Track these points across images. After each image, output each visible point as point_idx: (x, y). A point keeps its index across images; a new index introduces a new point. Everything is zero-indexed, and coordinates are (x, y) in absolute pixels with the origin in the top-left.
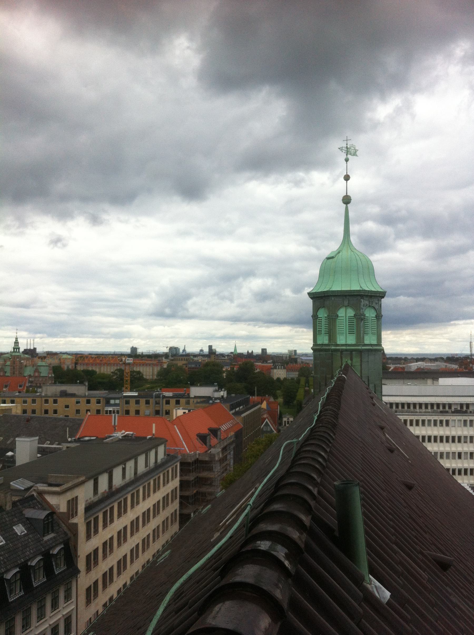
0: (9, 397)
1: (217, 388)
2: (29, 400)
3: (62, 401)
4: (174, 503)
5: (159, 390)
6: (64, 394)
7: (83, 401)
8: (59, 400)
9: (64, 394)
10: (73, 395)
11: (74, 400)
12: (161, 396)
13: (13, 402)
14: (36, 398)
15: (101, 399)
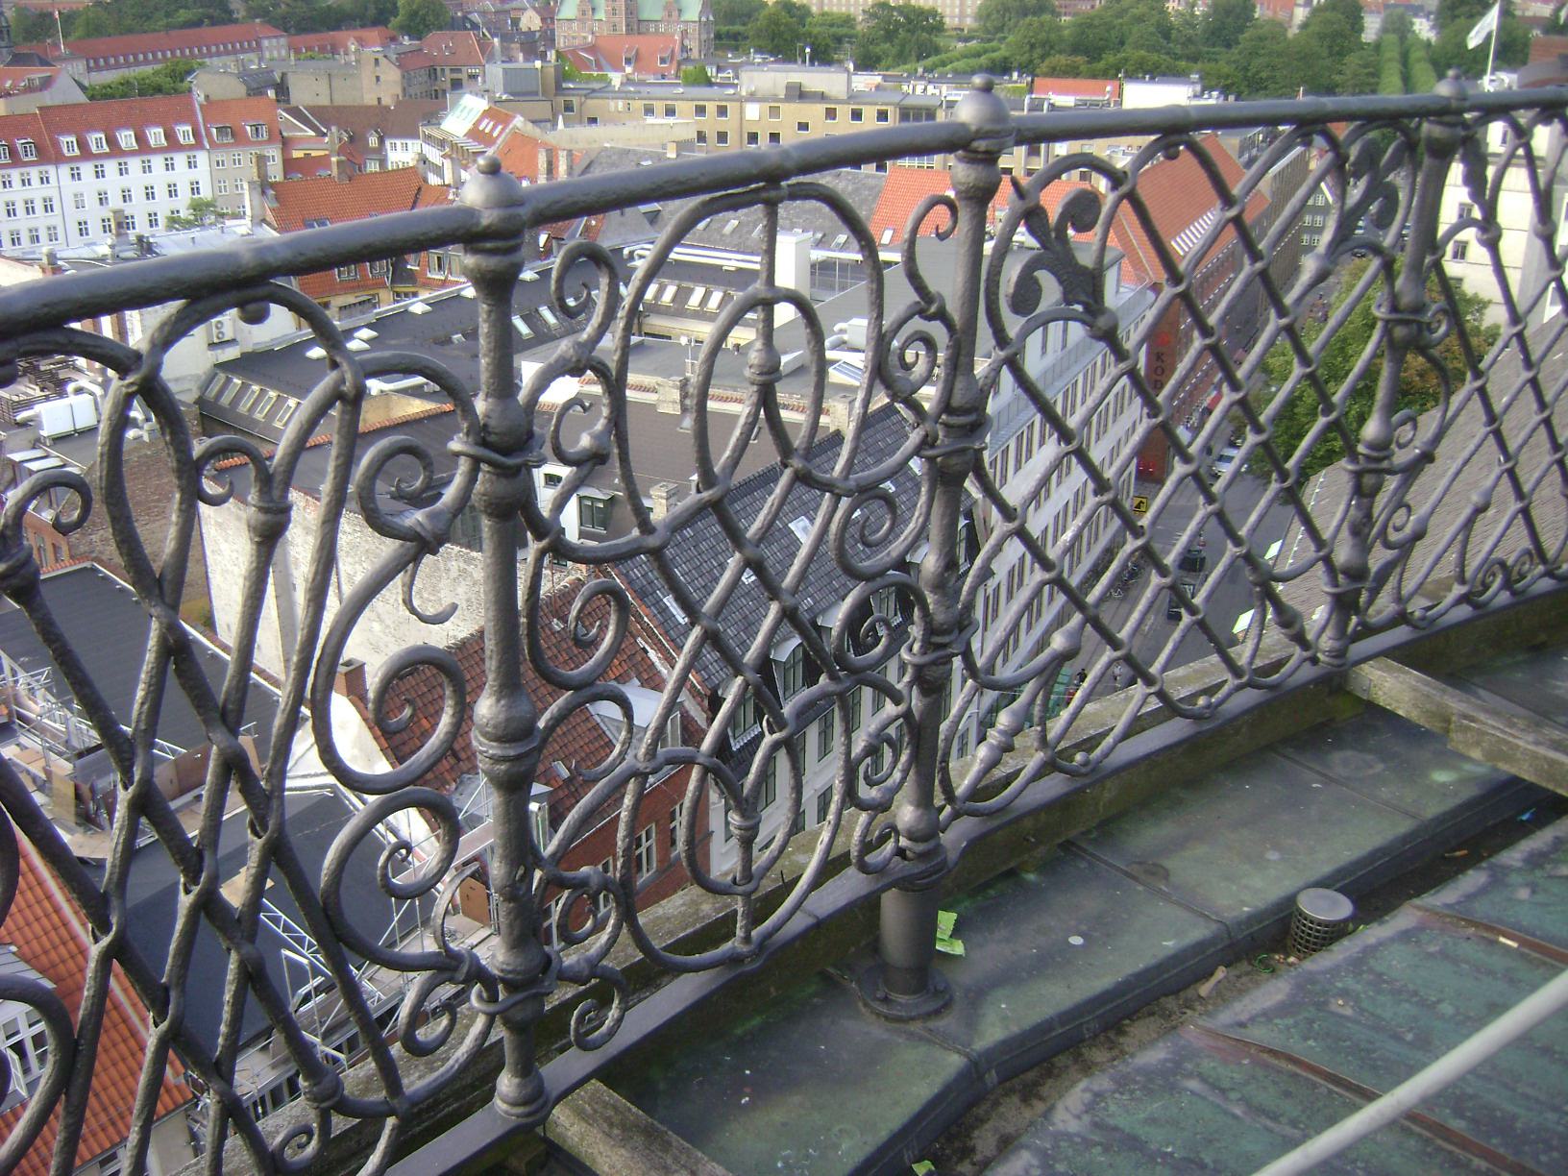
0: (661, 99)
1: (1198, 88)
2: (711, 107)
3: (793, 112)
4: (1133, 406)
5: (1015, 75)
6: (798, 94)
7: (844, 111)
8: (785, 108)
9: (798, 94)
10: (822, 97)
11: (820, 109)
12: (1046, 106)
13: (670, 112)
14: (728, 104)
15: (890, 109)
